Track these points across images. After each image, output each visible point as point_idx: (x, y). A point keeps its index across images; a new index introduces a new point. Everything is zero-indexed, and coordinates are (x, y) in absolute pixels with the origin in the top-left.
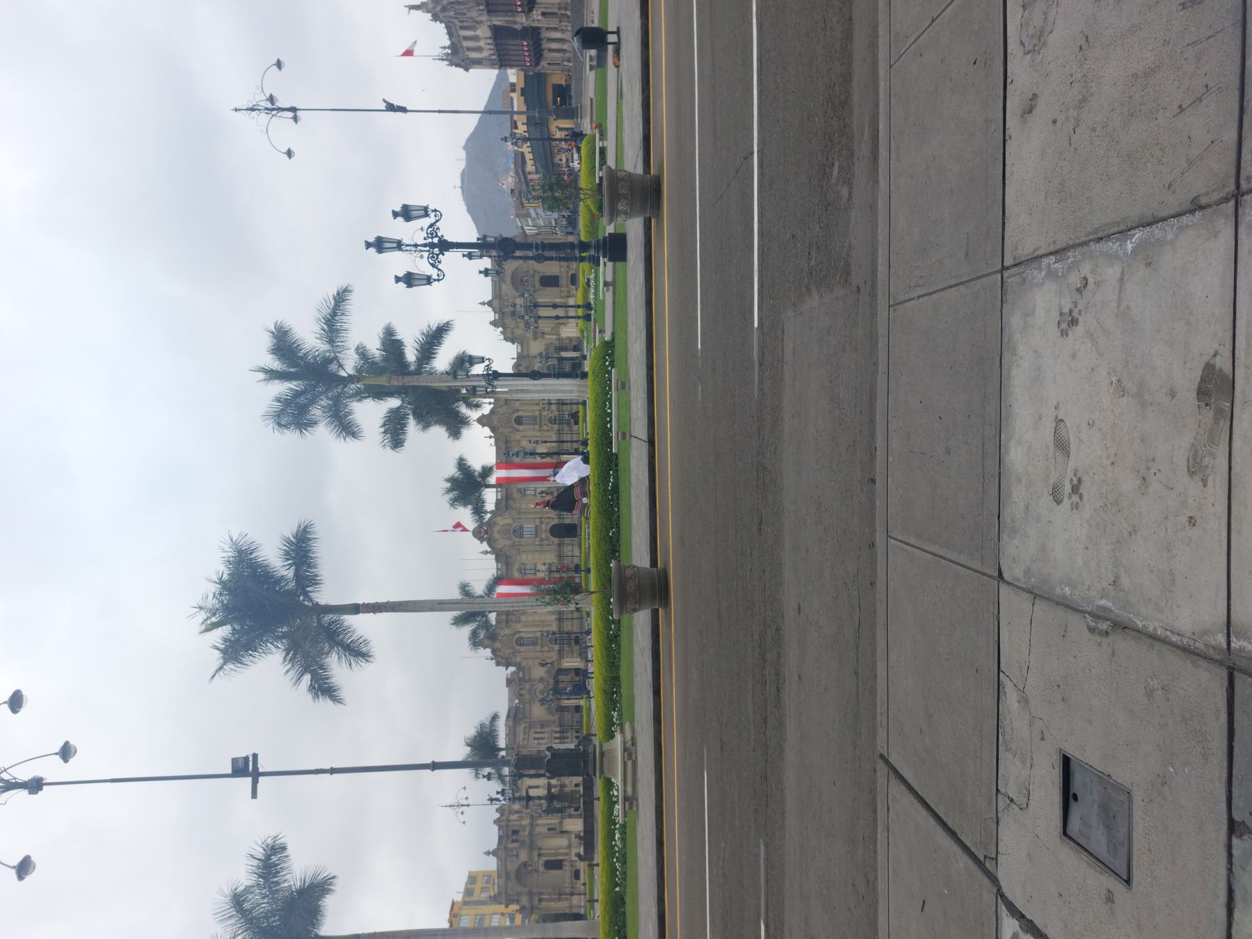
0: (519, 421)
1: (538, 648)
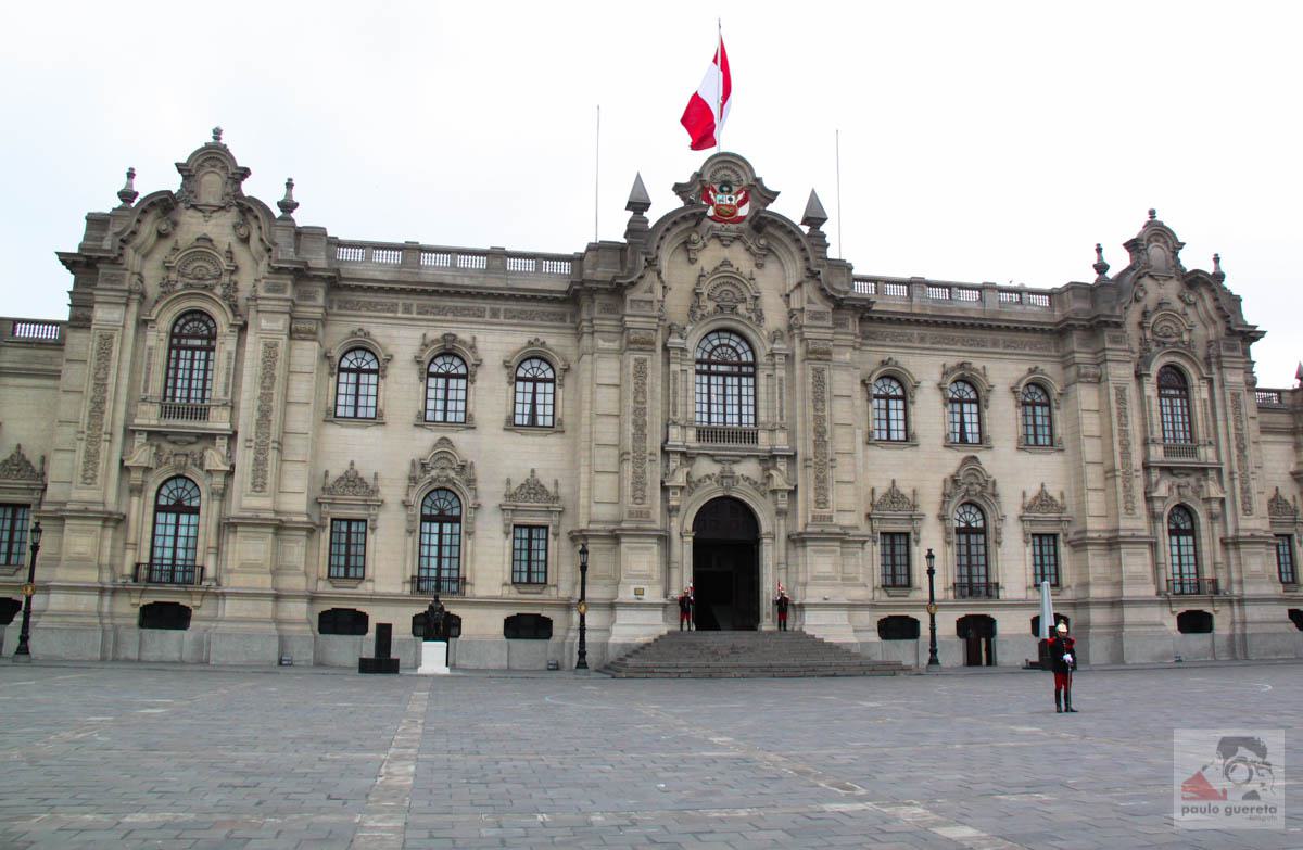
0: (1174, 381)
1: (149, 417)
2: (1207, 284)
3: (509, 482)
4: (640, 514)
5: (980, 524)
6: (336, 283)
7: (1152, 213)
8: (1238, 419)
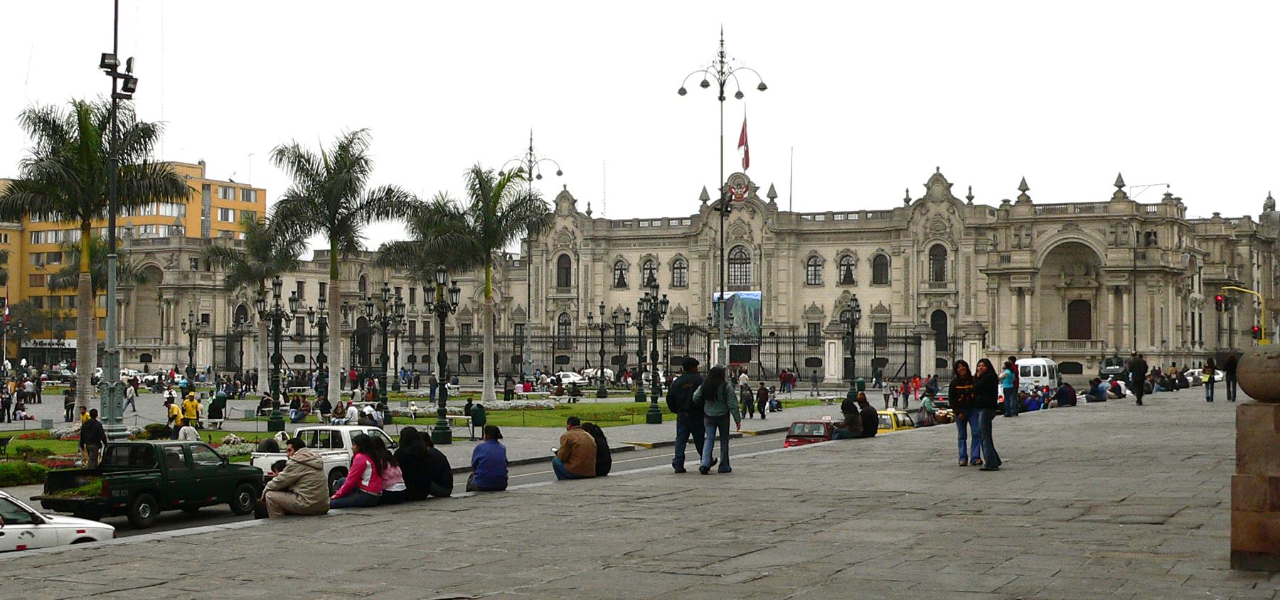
1: (553, 293)
6: (608, 240)
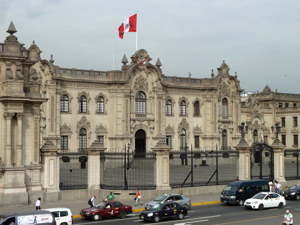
0: (225, 101)
2: (233, 78)
3: (96, 126)
4: (127, 134)
5: (185, 133)
7: (224, 61)
8: (237, 111)
